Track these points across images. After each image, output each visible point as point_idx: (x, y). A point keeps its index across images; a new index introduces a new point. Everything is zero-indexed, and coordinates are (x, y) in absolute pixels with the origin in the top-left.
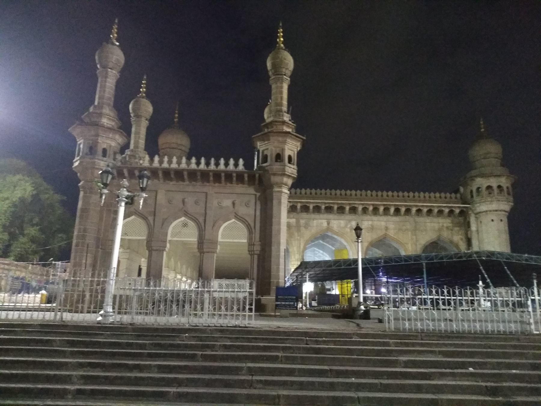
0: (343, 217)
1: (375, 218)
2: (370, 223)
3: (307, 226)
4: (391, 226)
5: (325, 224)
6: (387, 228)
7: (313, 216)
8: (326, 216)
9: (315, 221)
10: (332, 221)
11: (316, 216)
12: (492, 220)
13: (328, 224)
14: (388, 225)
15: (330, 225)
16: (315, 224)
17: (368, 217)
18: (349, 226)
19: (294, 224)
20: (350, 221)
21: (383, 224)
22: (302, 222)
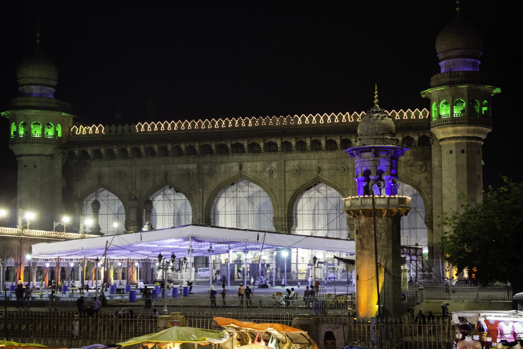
0: (259, 157)
1: (303, 156)
2: (296, 163)
3: (212, 173)
4: (325, 166)
5: (236, 168)
6: (319, 170)
7: (219, 158)
8: (237, 157)
9: (223, 166)
10: (245, 164)
11: (225, 158)
12: (451, 152)
13: (241, 168)
14: (319, 165)
15: (243, 170)
16: (223, 169)
17: (294, 155)
18: (268, 169)
19: (196, 171)
20: (270, 162)
21: (314, 162)
22: (206, 167)
